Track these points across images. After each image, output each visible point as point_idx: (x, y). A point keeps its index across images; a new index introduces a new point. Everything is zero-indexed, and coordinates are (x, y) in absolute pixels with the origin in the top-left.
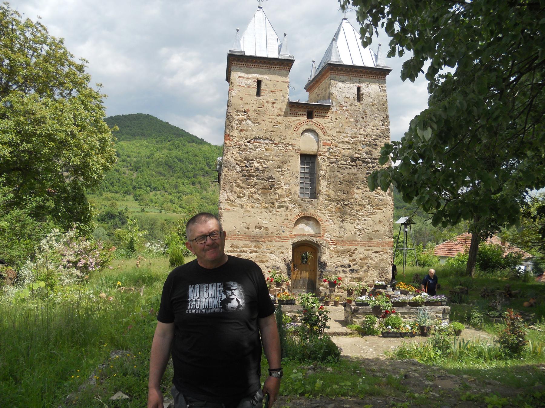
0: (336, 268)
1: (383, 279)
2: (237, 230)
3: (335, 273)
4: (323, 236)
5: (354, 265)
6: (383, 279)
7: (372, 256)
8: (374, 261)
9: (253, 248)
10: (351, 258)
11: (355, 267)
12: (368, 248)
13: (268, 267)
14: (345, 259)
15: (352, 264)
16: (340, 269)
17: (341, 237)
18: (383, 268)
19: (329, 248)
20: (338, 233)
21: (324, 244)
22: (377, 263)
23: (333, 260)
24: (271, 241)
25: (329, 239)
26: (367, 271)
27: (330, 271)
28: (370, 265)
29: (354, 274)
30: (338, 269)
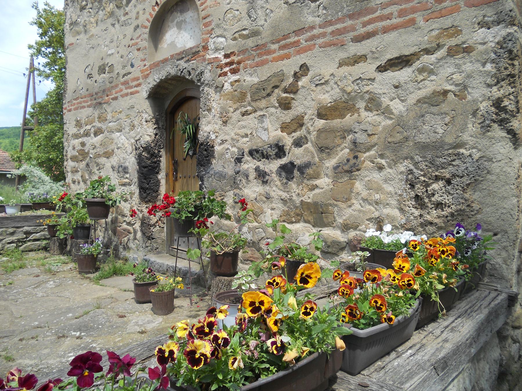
0: (239, 160)
1: (433, 215)
2: (80, 88)
3: (235, 184)
4: (205, 48)
5: (298, 143)
6: (433, 215)
7: (376, 88)
8: (387, 112)
9: (98, 124)
10: (287, 116)
11: (297, 155)
12: (355, 49)
13: (113, 168)
14: (267, 123)
15: (288, 140)
16: (250, 165)
17: (255, 33)
18: (437, 146)
19: (219, 88)
20: (246, 22)
21: (207, 76)
22: (400, 123)
23: (231, 132)
24: (116, 99)
25: (220, 55)
26: (349, 170)
27: (221, 176)
28: (361, 138)
29: (293, 185)
30: (244, 166)
